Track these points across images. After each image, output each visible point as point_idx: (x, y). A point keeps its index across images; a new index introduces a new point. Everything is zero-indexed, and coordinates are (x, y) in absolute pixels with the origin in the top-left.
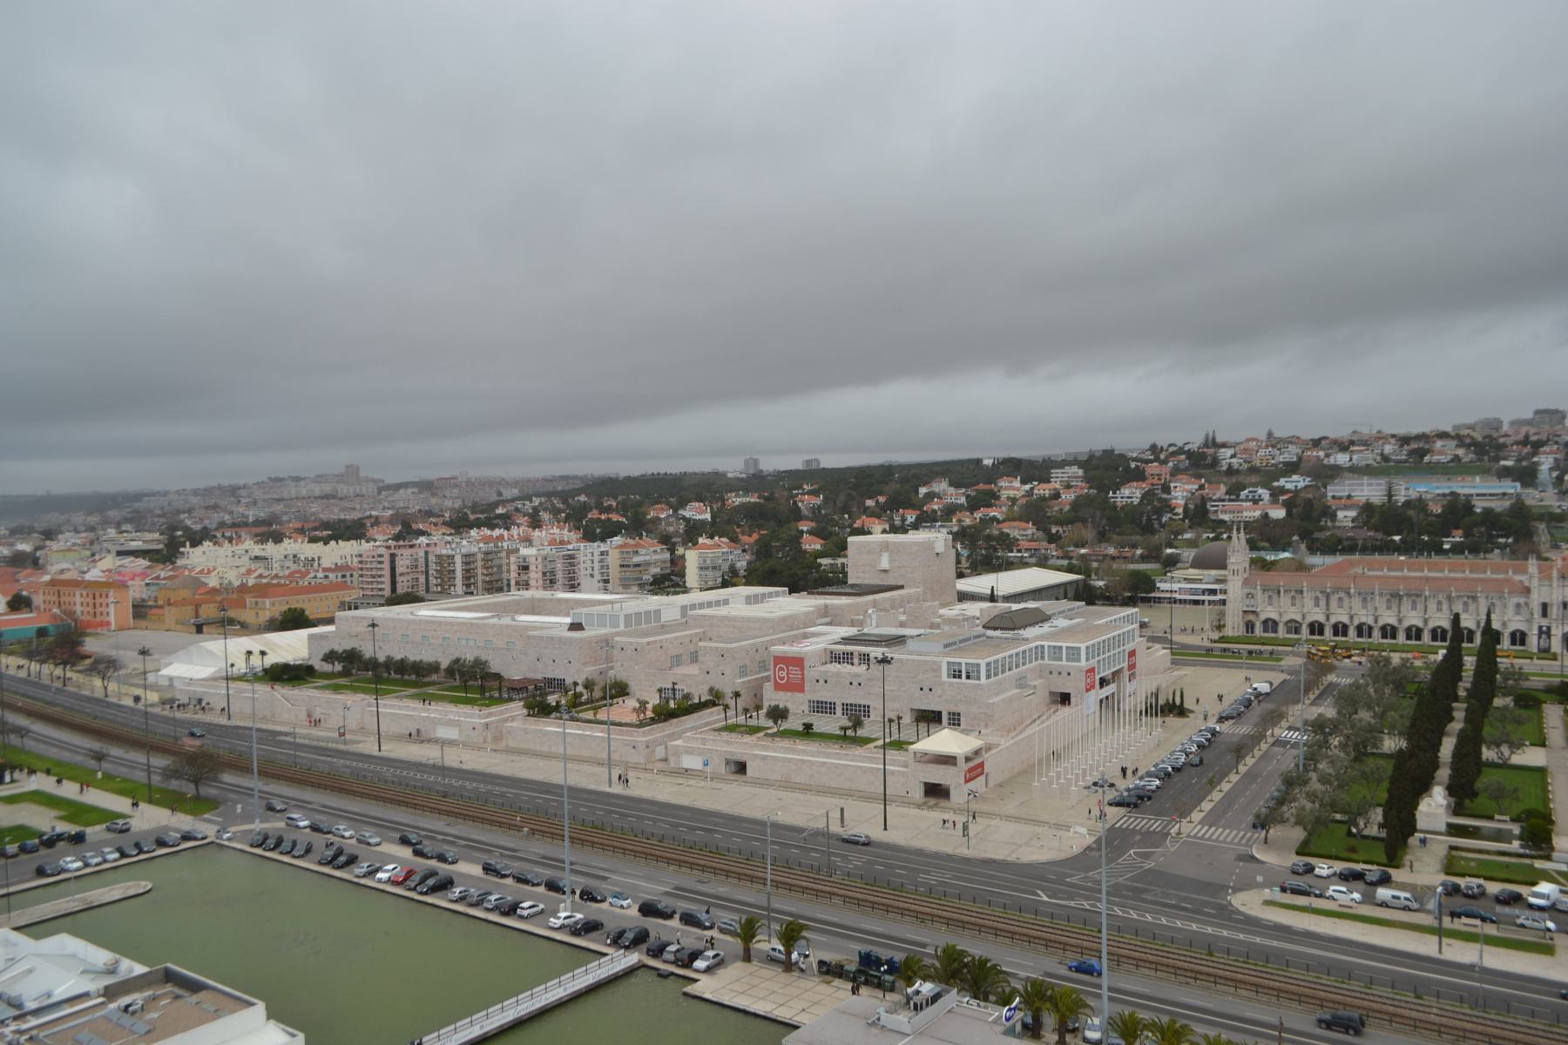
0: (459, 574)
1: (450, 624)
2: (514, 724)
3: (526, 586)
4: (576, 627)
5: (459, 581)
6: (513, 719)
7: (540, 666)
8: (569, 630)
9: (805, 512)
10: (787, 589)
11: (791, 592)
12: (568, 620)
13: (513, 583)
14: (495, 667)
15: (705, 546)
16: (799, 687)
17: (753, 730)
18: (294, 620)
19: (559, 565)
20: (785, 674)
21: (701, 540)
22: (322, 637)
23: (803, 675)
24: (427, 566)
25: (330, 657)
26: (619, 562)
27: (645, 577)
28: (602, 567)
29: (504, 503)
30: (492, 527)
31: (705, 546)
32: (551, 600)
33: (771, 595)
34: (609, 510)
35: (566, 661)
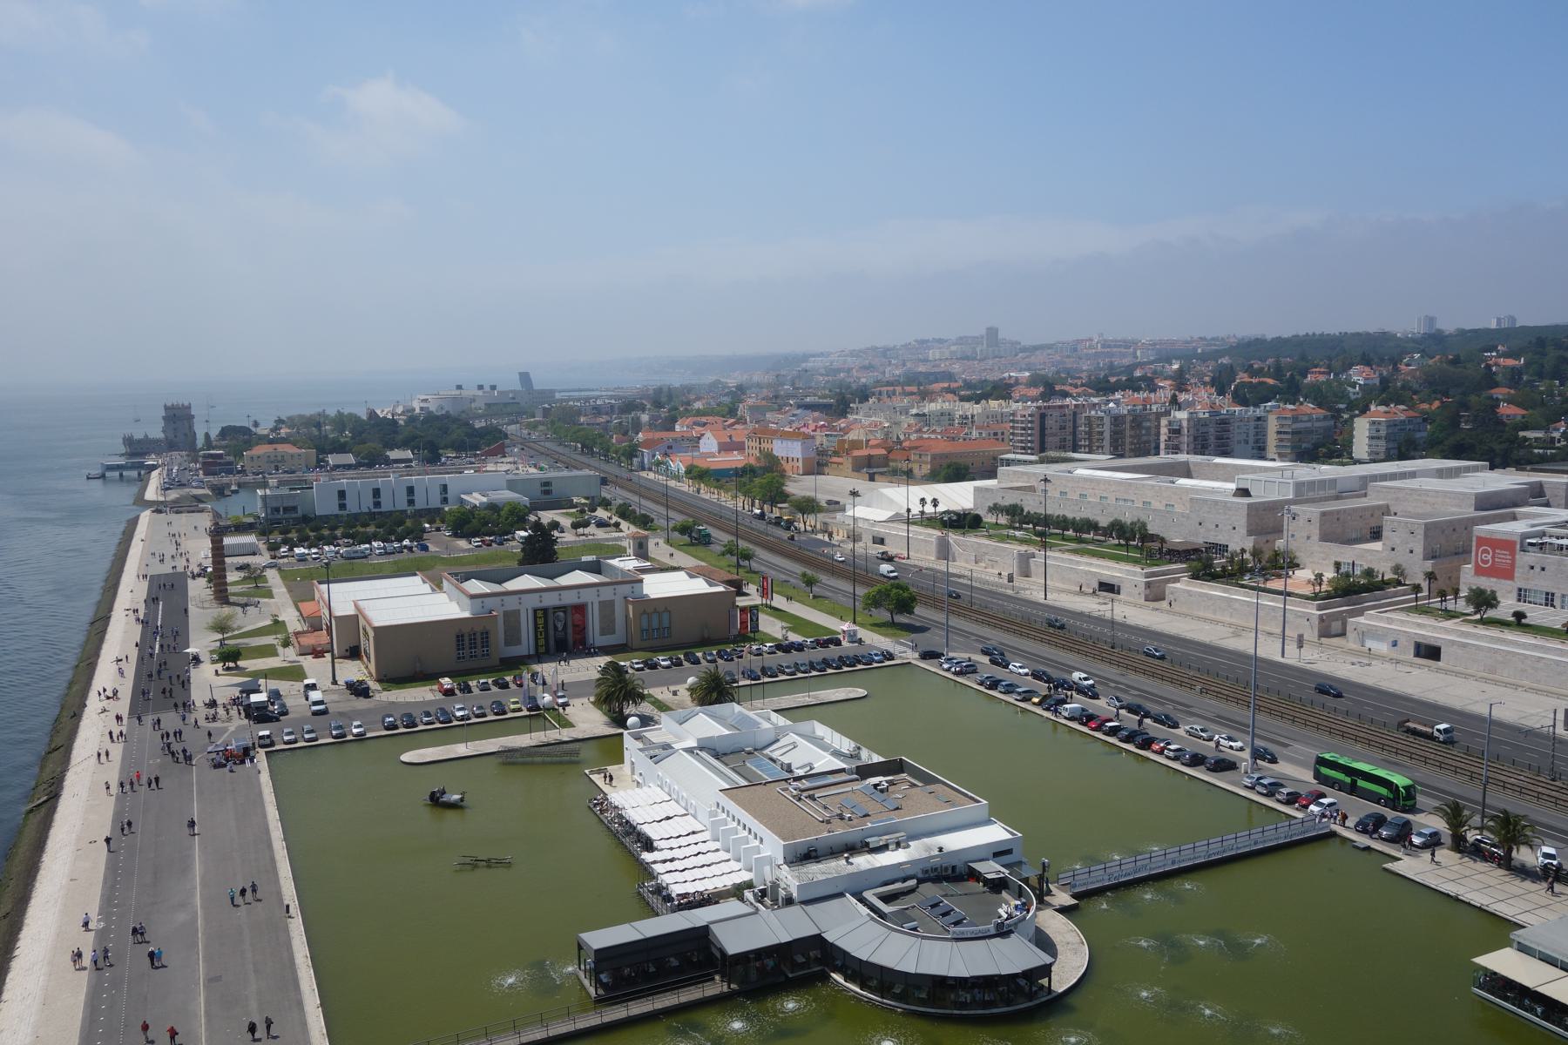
0: (1107, 435)
1: (1108, 482)
2: (1178, 585)
3: (1176, 449)
4: (1244, 492)
5: (1107, 443)
6: (1177, 580)
7: (1202, 530)
8: (1235, 495)
9: (1499, 378)
10: (1488, 463)
11: (1492, 468)
12: (1232, 486)
13: (1162, 446)
14: (1152, 529)
15: (1377, 414)
16: (1507, 573)
17: (1450, 615)
18: (957, 473)
19: (1212, 430)
20: (1489, 557)
21: (1373, 408)
22: (987, 490)
23: (1513, 560)
24: (1075, 427)
25: (995, 509)
26: (1275, 429)
27: (1304, 445)
28: (1257, 434)
29: (1141, 365)
30: (1137, 389)
31: (1377, 414)
32: (1209, 465)
33: (1467, 470)
34: (1259, 373)
35: (1231, 527)
